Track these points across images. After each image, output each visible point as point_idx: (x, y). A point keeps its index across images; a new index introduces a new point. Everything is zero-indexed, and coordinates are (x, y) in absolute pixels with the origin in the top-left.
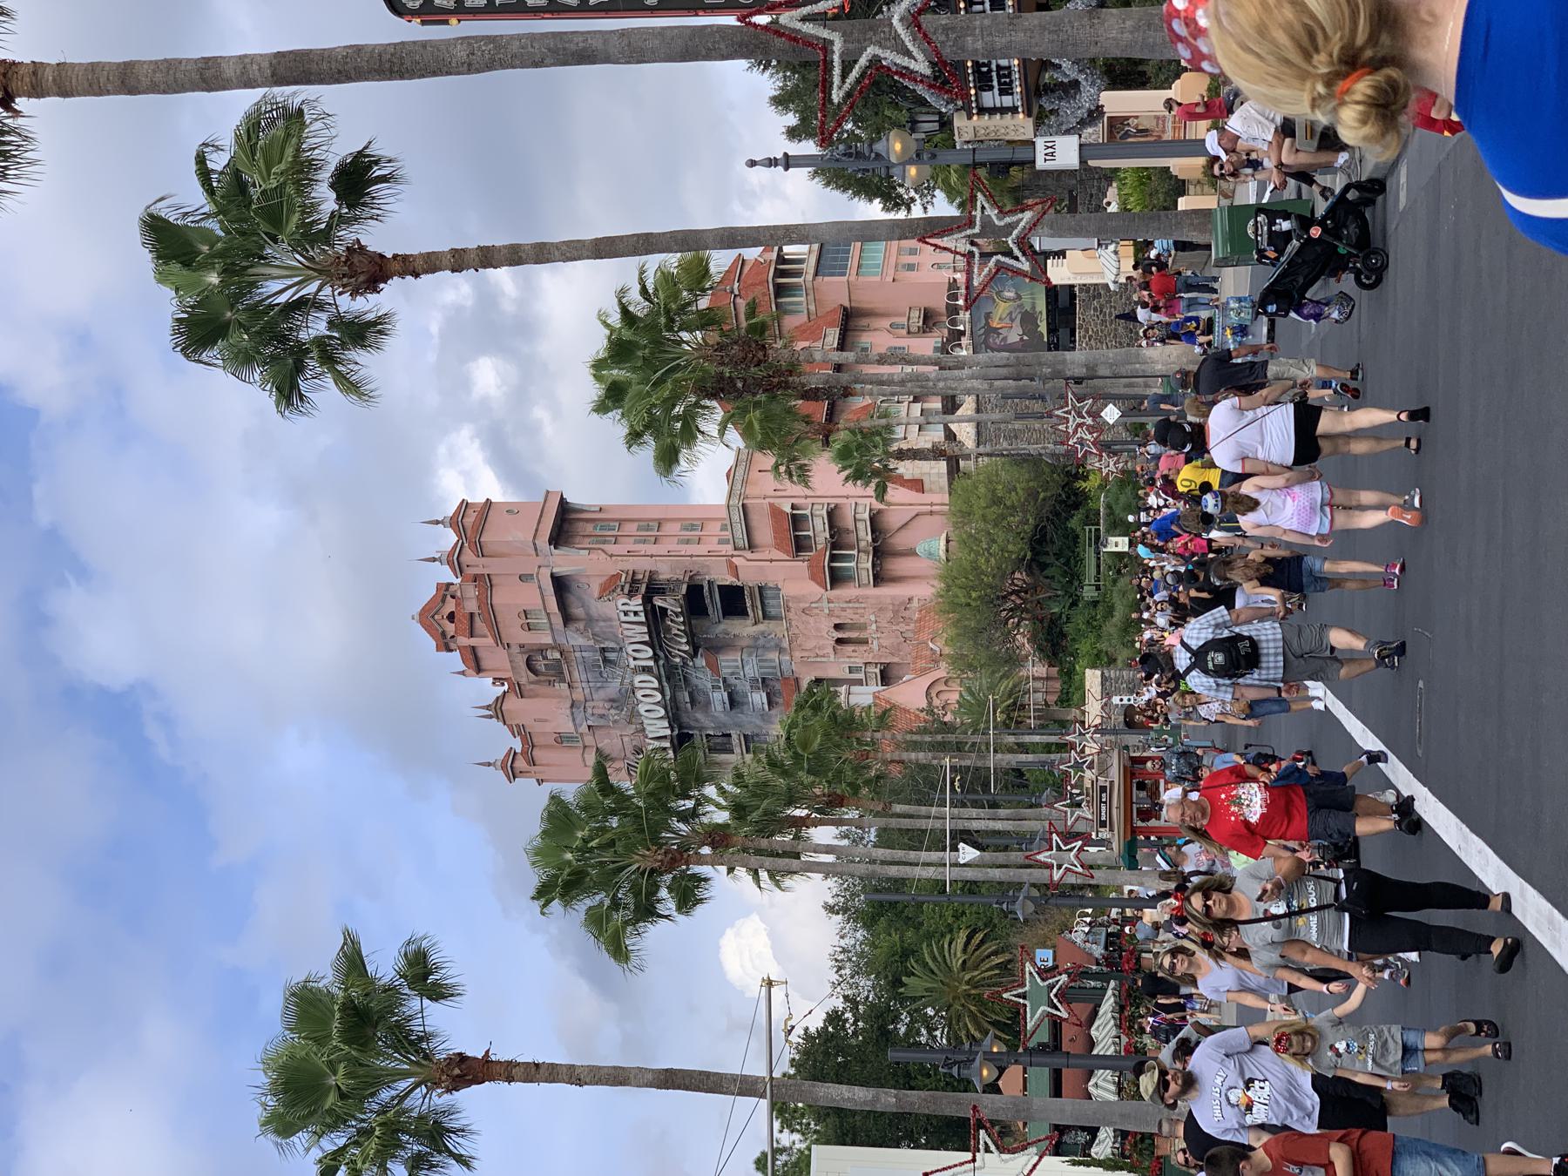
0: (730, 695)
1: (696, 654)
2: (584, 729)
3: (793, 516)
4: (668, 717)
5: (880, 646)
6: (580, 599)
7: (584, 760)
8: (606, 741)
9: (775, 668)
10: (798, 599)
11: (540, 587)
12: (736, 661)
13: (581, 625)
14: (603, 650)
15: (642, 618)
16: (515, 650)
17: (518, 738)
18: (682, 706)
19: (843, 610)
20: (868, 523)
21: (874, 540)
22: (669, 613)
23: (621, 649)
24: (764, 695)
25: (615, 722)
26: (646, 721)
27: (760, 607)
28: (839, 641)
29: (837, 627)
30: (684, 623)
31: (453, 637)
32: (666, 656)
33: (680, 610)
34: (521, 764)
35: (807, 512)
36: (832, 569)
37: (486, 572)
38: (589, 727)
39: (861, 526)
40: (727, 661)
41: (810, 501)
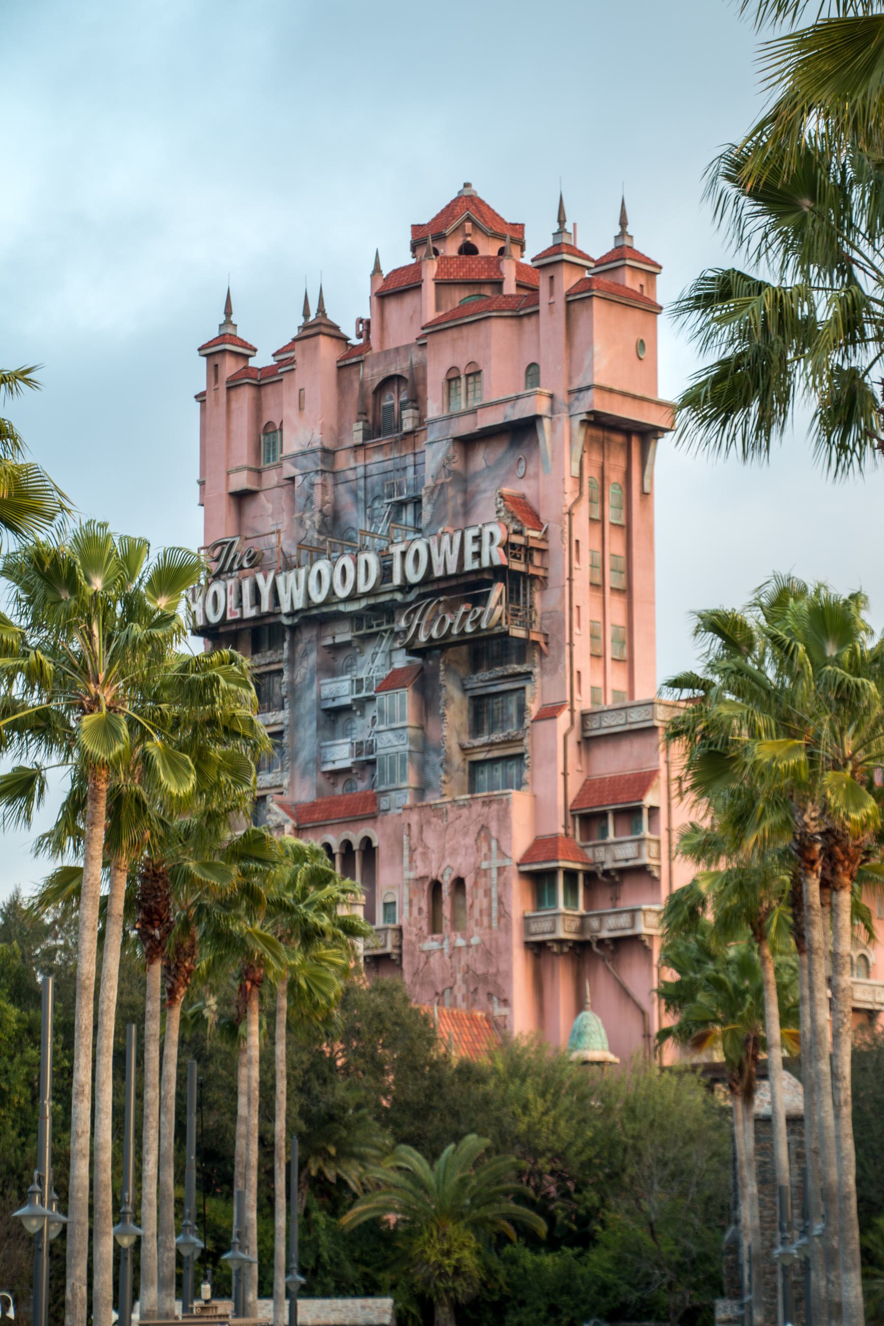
0: (345, 709)
1: (411, 650)
2: (289, 470)
3: (638, 810)
4: (309, 609)
5: (429, 954)
6: (499, 463)
7: (238, 470)
8: (269, 506)
9: (392, 781)
11: (518, 398)
12: (403, 718)
13: (457, 465)
14: (417, 502)
15: (470, 565)
16: (416, 356)
17: (271, 362)
18: (329, 631)
19: (487, 893)
20: (629, 932)
21: (601, 942)
22: (479, 610)
23: (419, 530)
24: (347, 764)
25: (301, 522)
26: (302, 572)
27: (490, 755)
28: (436, 886)
29: (459, 883)
30: (462, 633)
31: (436, 252)
32: (409, 604)
33: (484, 626)
34: (230, 367)
35: (646, 832)
36: (552, 873)
37: (543, 307)
38: (292, 479)
39: (624, 920)
40: (402, 703)
41: (663, 836)
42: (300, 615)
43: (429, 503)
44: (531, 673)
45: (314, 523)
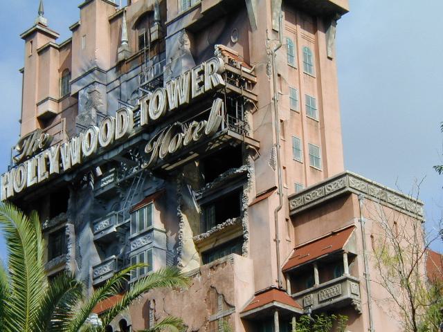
10: (228, 281)
42: (78, 171)
44: (247, 172)
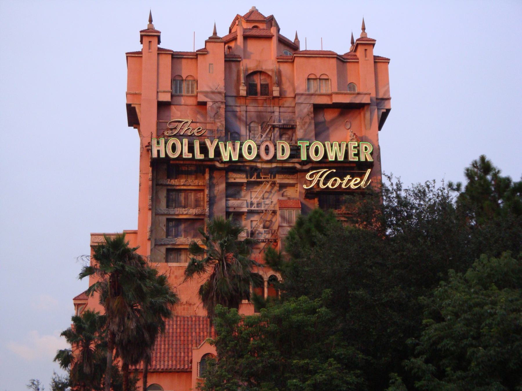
43: (301, 128)
45: (222, 124)
